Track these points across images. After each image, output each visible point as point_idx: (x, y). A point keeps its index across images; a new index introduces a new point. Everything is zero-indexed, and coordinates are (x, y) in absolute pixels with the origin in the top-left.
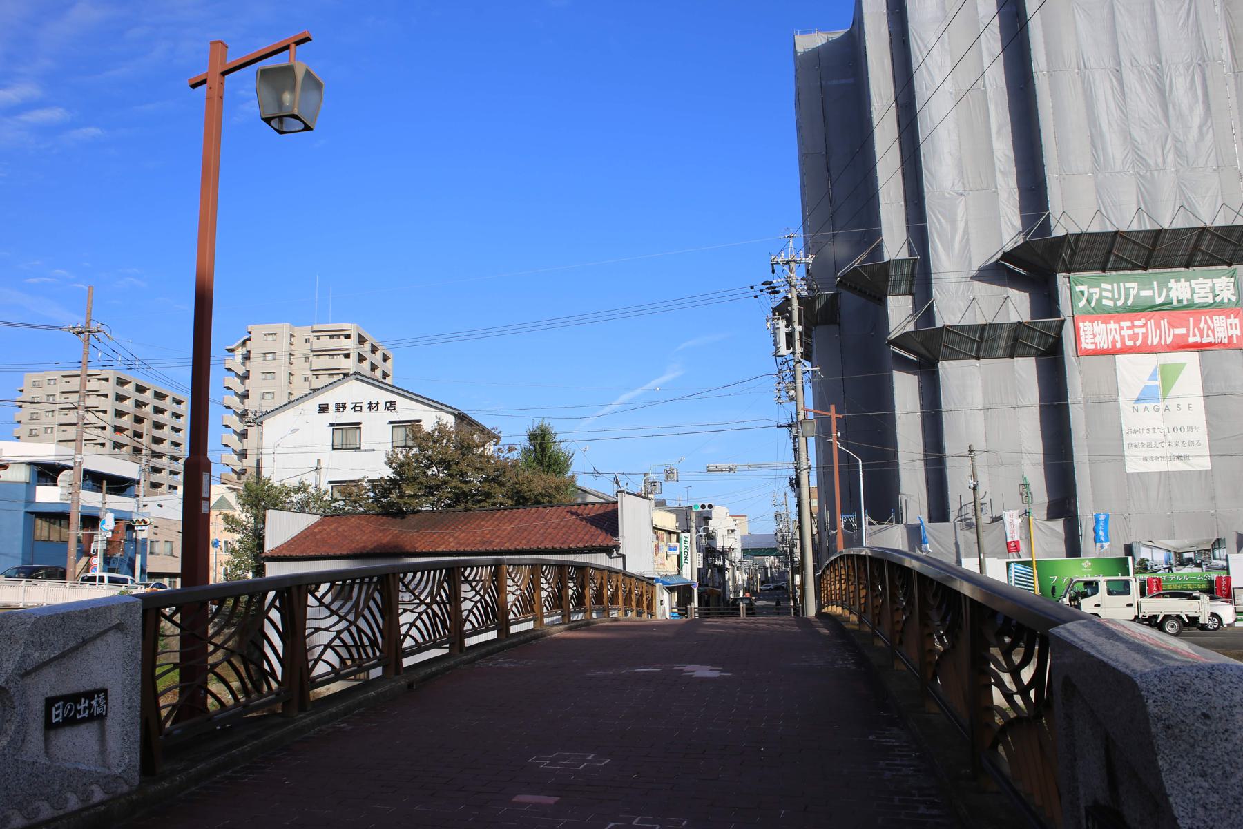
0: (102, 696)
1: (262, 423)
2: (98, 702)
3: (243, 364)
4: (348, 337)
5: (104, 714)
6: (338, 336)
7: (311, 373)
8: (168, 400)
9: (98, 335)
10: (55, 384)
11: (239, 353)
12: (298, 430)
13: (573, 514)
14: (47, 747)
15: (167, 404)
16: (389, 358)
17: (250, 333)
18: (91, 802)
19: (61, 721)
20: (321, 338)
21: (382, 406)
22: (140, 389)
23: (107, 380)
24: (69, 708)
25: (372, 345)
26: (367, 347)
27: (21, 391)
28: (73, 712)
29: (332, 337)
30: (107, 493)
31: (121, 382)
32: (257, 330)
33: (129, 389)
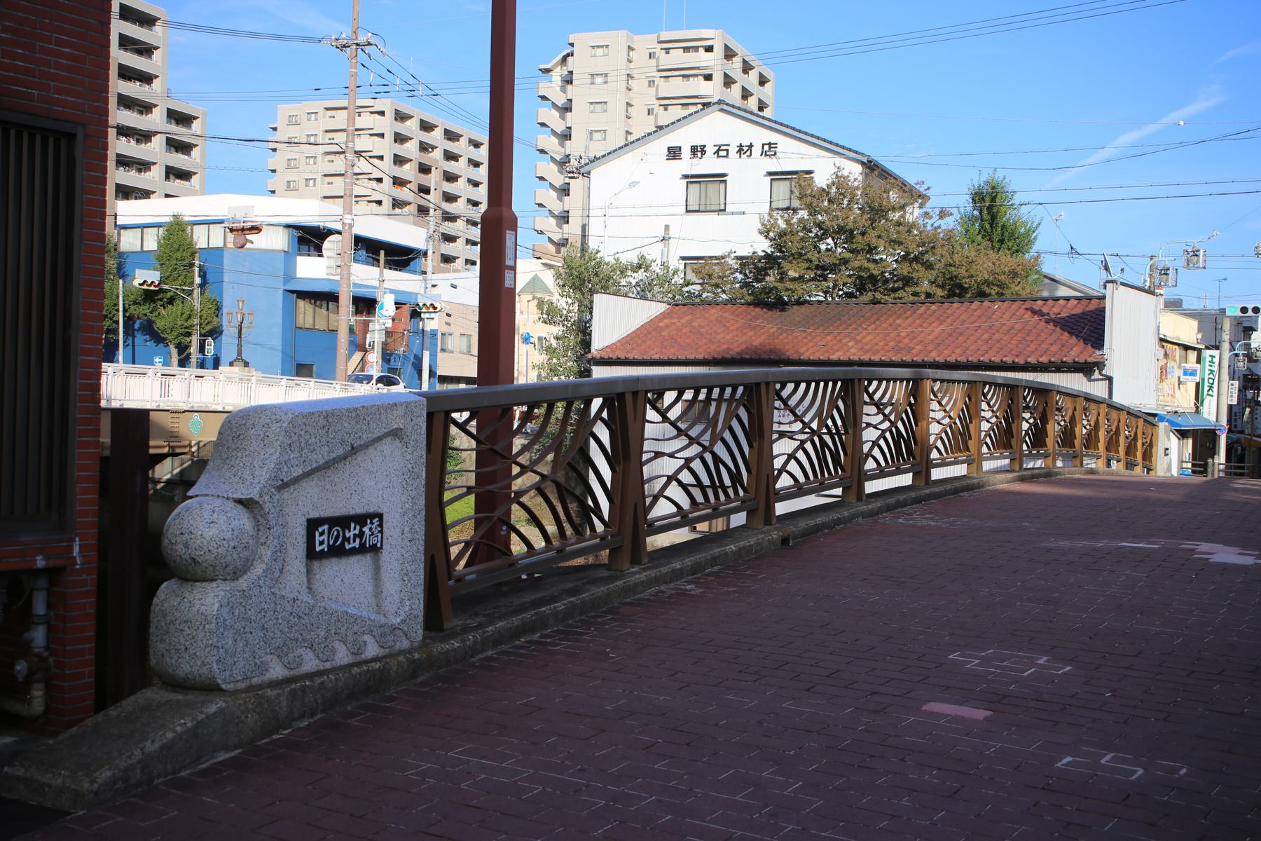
0: (376, 521)
1: (589, 173)
2: (371, 529)
3: (563, 90)
4: (709, 49)
5: (379, 545)
6: (696, 49)
7: (658, 102)
8: (463, 141)
9: (368, 49)
10: (316, 119)
11: (557, 75)
12: (638, 183)
13: (1034, 312)
14: (309, 581)
15: (461, 147)
16: (769, 81)
17: (572, 45)
18: (363, 656)
19: (326, 550)
20: (671, 51)
21: (757, 150)
22: (426, 127)
23: (382, 113)
24: (335, 533)
25: (744, 61)
26: (737, 63)
27: (275, 129)
28: (340, 540)
29: (686, 49)
30: (385, 268)
31: (401, 117)
32: (582, 41)
33: (411, 127)
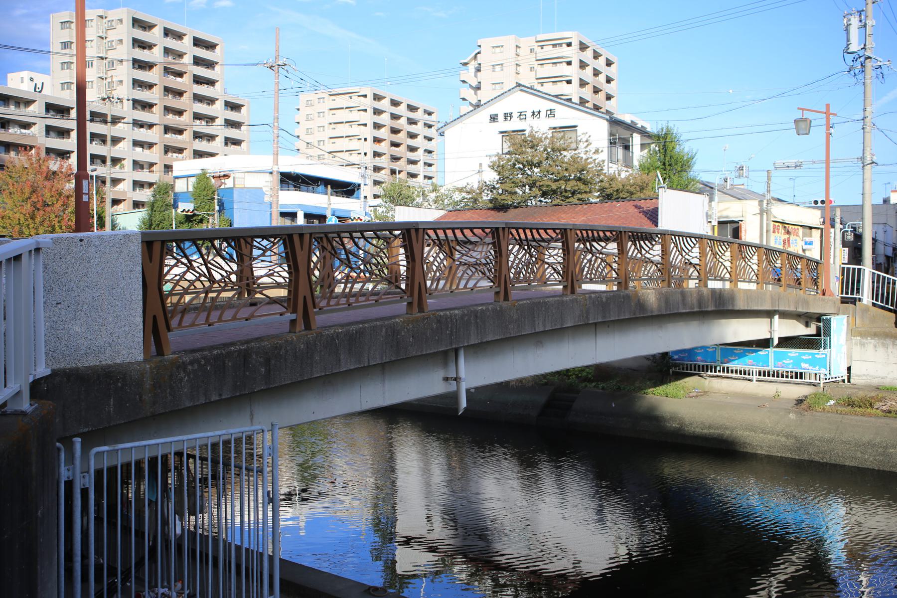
3: (476, 76)
4: (569, 45)
6: (561, 45)
7: (537, 81)
8: (420, 112)
10: (324, 102)
11: (472, 66)
15: (419, 115)
16: (613, 63)
17: (480, 46)
20: (544, 47)
22: (395, 103)
23: (365, 96)
25: (594, 51)
26: (589, 53)
27: (298, 109)
29: (554, 46)
31: (377, 98)
32: (486, 43)
33: (385, 104)
